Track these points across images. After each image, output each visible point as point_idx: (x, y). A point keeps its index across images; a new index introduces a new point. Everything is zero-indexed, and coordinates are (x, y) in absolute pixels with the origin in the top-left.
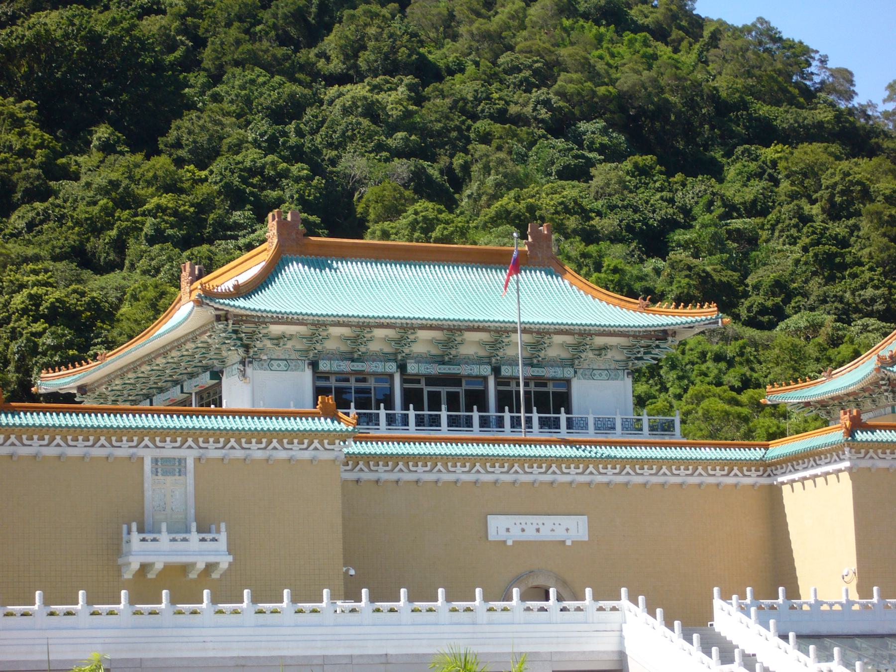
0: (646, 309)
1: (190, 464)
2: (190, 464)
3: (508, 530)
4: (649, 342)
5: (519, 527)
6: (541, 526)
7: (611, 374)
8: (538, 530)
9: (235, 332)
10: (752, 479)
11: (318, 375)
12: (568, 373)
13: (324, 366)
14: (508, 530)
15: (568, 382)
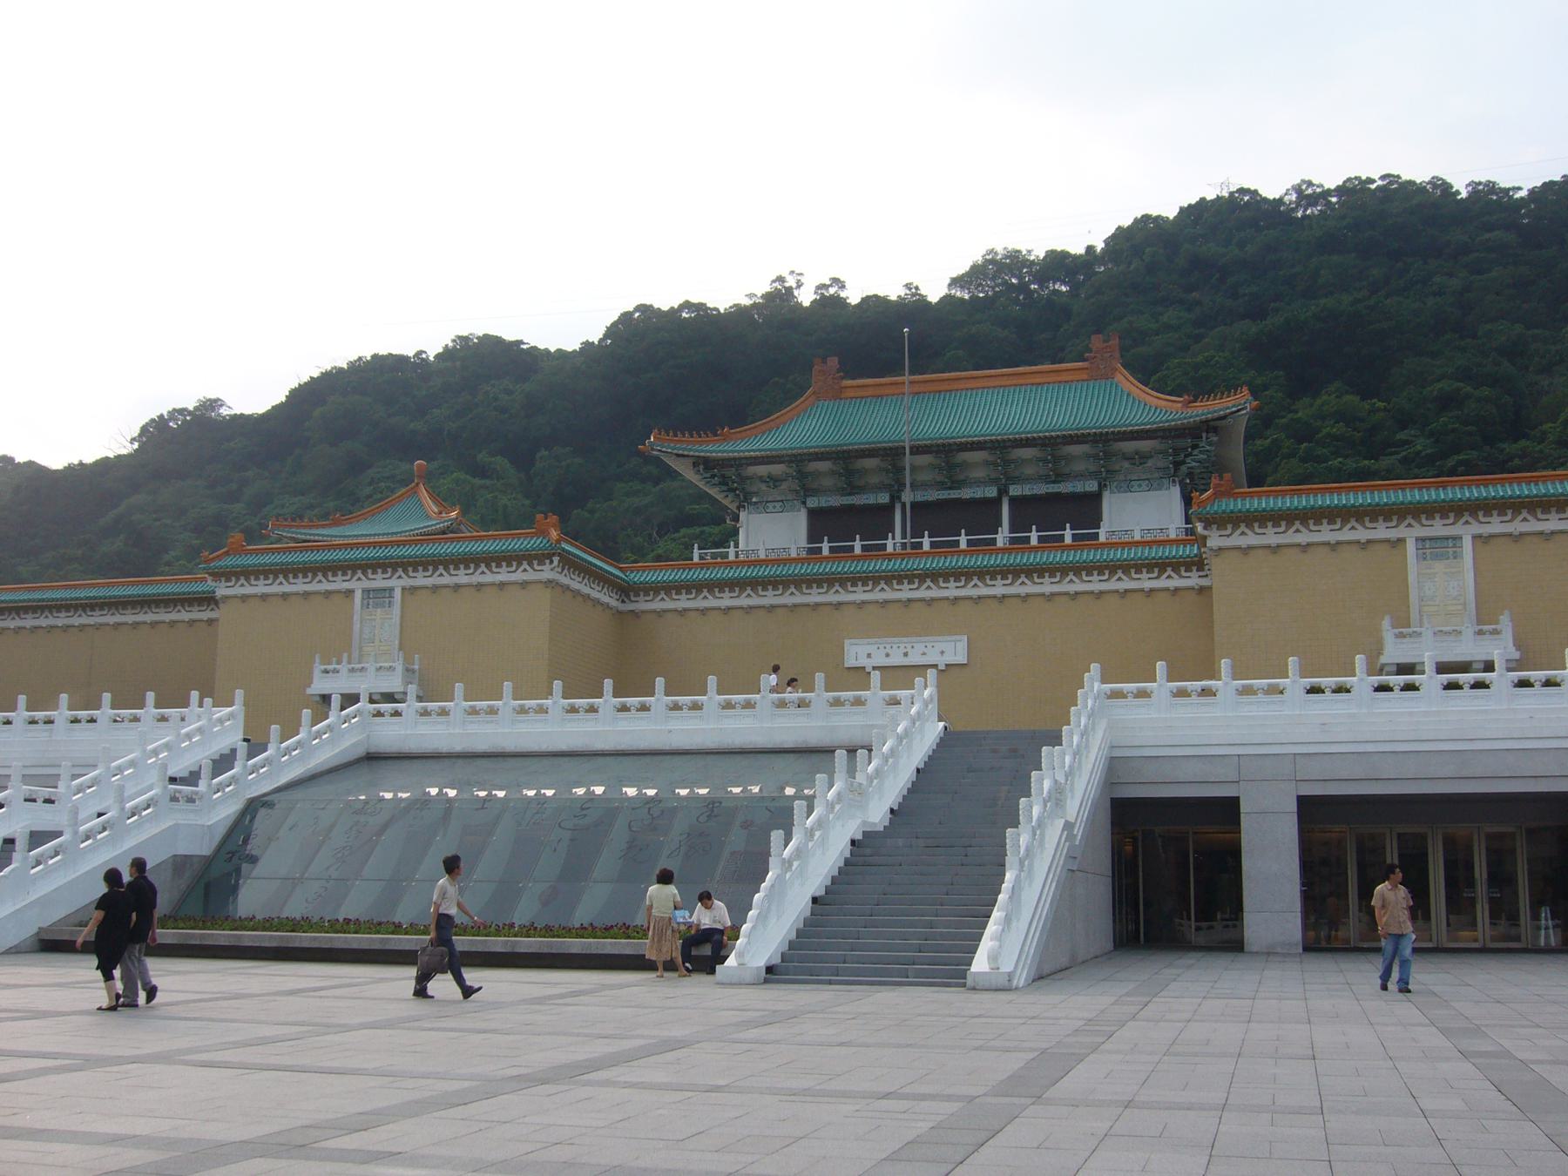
0: (1187, 404)
1: (398, 593)
2: (398, 593)
3: (869, 656)
4: (1181, 443)
5: (883, 652)
6: (909, 650)
7: (1153, 484)
8: (906, 654)
9: (713, 476)
10: (1193, 580)
11: (813, 514)
12: (1092, 486)
13: (813, 502)
14: (869, 656)
15: (1094, 499)
